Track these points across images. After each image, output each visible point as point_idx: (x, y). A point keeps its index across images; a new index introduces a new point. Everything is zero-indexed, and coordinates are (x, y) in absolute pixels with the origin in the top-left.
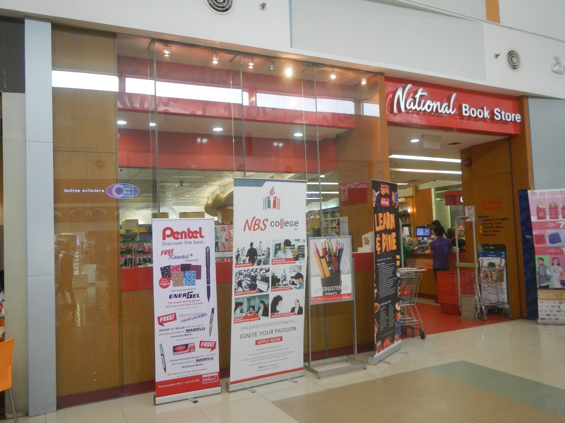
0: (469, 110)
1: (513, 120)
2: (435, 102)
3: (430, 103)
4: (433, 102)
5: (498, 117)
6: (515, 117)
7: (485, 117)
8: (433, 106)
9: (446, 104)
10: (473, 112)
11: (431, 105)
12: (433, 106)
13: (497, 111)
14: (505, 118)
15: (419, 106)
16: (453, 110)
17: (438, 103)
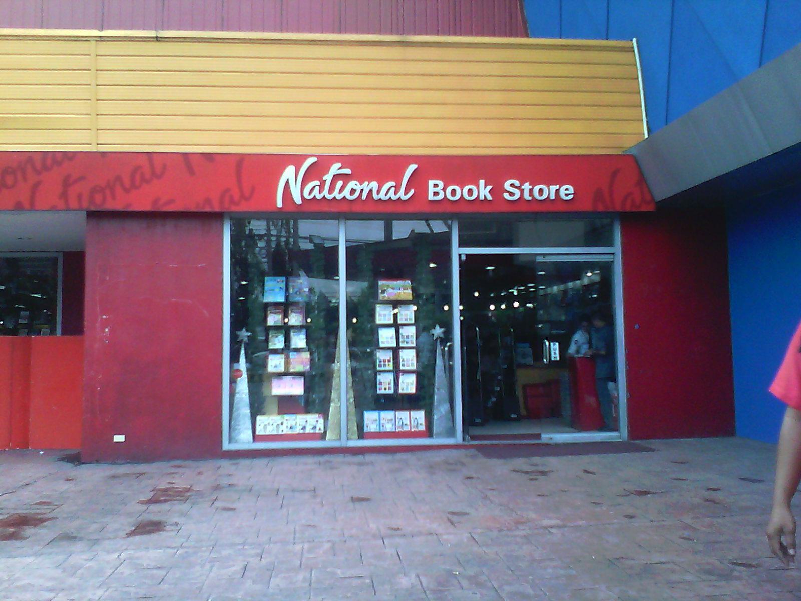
0: (444, 189)
1: (552, 197)
2: (366, 183)
6: (557, 191)
7: (481, 198)
8: (362, 191)
9: (393, 184)
10: (453, 192)
11: (358, 188)
12: (362, 191)
13: (512, 185)
15: (331, 190)
16: (405, 194)
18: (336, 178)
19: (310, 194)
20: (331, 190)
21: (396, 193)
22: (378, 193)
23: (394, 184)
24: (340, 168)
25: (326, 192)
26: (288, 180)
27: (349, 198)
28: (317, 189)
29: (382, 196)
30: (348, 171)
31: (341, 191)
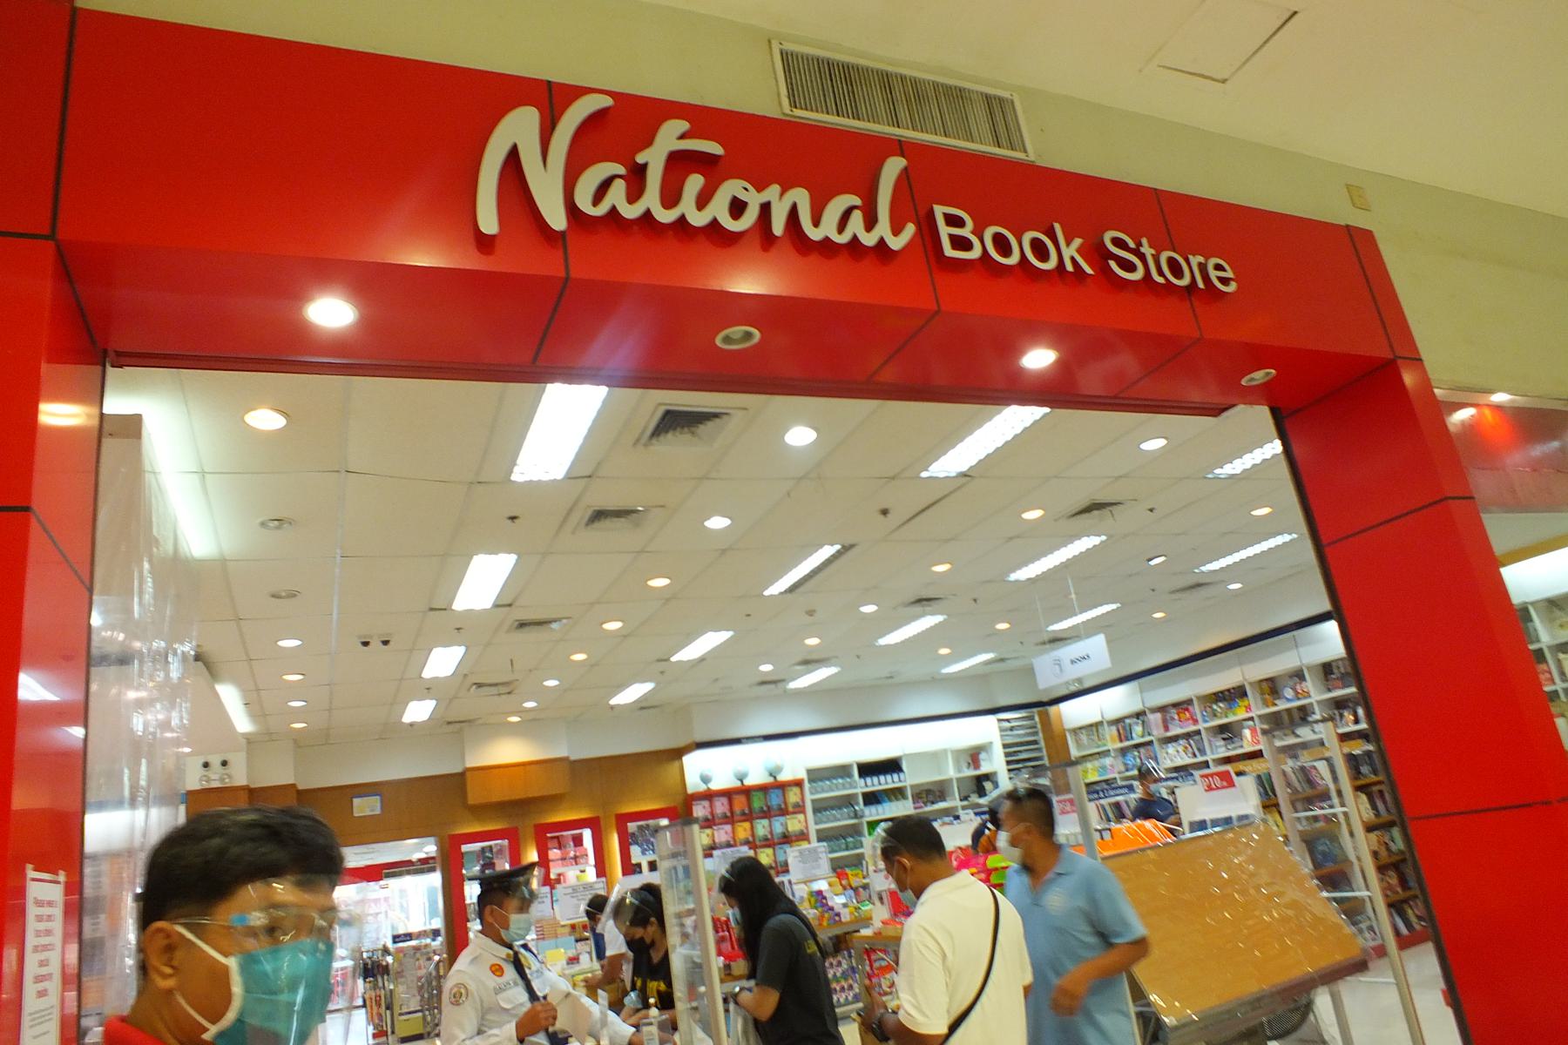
3: (746, 189)
5: (1130, 267)
8: (766, 208)
10: (1002, 245)
12: (766, 208)
13: (1118, 242)
14: (1161, 273)
15: (670, 198)
18: (680, 163)
19: (599, 195)
24: (683, 137)
25: (651, 199)
29: (827, 229)
31: (702, 201)
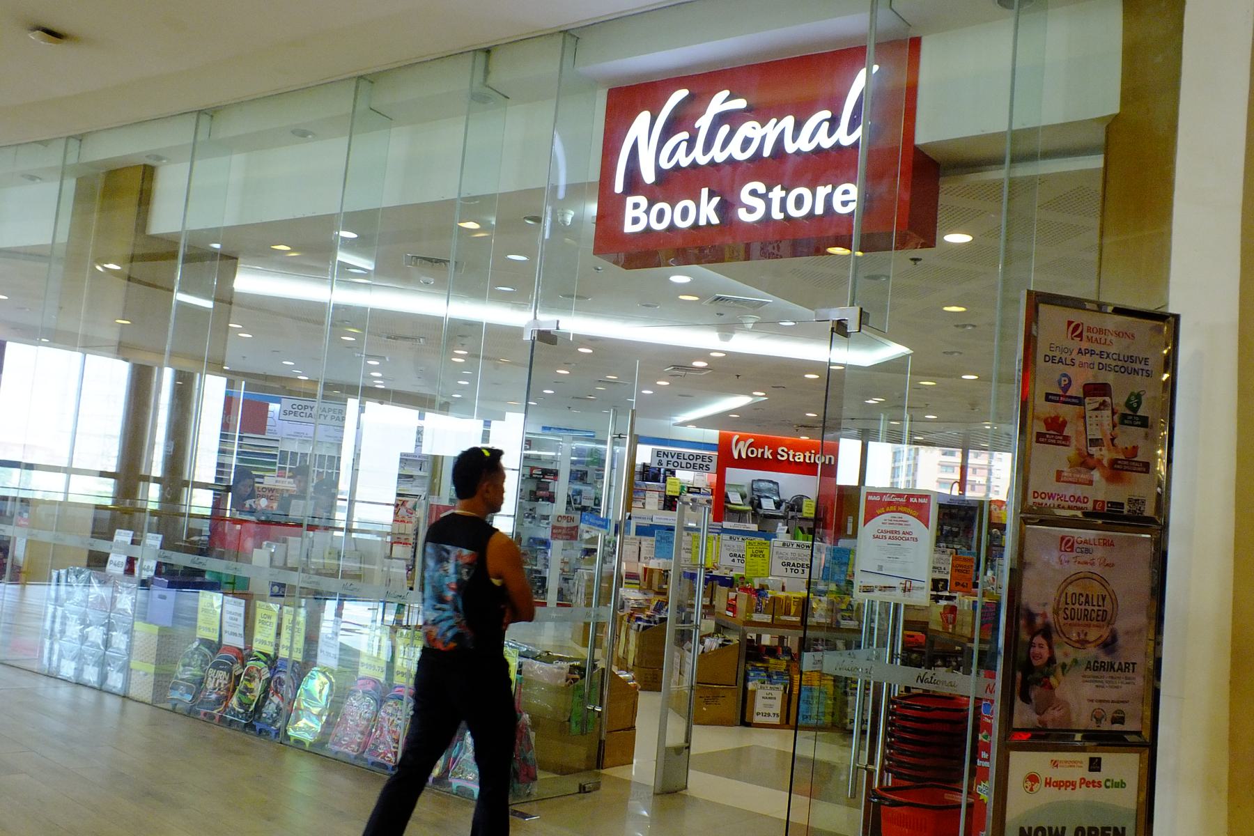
2: (774, 121)
3: (754, 128)
4: (763, 126)
8: (763, 138)
9: (827, 114)
12: (763, 138)
15: (708, 147)
16: (851, 131)
17: (789, 122)
18: (721, 119)
19: (670, 159)
20: (708, 147)
21: (831, 132)
22: (795, 139)
23: (827, 114)
26: (637, 138)
27: (741, 156)
28: (684, 145)
29: (805, 145)
30: (740, 104)
